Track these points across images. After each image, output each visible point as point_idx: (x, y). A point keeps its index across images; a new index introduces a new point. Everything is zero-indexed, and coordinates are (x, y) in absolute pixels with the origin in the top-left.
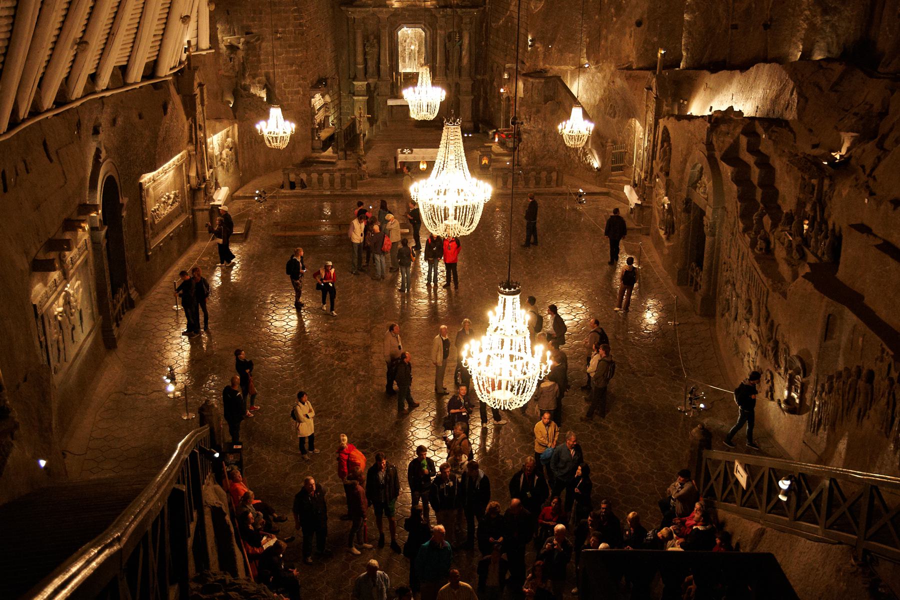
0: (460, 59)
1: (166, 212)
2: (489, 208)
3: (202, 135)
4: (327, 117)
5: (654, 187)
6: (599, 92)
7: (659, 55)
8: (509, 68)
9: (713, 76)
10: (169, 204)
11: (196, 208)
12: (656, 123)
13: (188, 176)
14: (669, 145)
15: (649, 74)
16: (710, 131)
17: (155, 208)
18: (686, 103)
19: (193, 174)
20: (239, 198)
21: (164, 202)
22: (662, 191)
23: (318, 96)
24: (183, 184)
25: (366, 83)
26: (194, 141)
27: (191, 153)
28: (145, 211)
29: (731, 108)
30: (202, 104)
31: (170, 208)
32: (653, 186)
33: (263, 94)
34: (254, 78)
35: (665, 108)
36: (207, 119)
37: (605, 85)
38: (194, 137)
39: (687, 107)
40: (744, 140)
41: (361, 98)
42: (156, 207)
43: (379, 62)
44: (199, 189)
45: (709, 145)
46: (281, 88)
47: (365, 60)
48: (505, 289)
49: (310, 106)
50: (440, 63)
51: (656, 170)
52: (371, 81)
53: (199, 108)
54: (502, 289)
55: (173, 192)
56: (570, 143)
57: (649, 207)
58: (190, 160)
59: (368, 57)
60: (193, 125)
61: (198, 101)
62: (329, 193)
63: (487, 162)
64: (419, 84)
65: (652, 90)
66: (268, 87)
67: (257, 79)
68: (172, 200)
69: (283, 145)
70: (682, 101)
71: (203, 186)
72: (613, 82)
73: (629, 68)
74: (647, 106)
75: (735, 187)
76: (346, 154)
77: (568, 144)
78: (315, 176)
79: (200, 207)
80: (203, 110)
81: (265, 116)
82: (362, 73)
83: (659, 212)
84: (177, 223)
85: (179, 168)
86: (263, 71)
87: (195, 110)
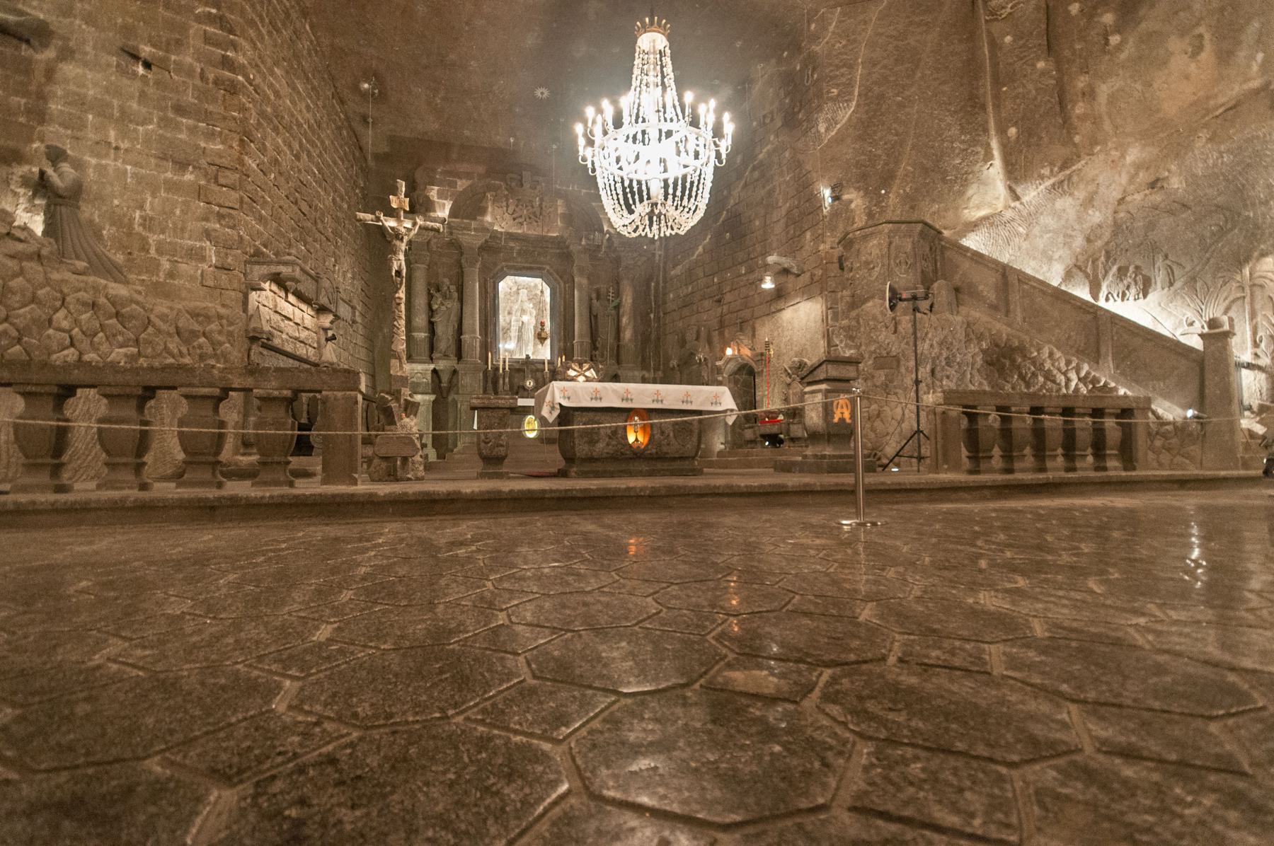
0: (618, 331)
25: (432, 366)
43: (460, 331)
46: (130, 226)
49: (245, 310)
50: (581, 336)
52: (441, 365)
59: (436, 319)
82: (425, 347)
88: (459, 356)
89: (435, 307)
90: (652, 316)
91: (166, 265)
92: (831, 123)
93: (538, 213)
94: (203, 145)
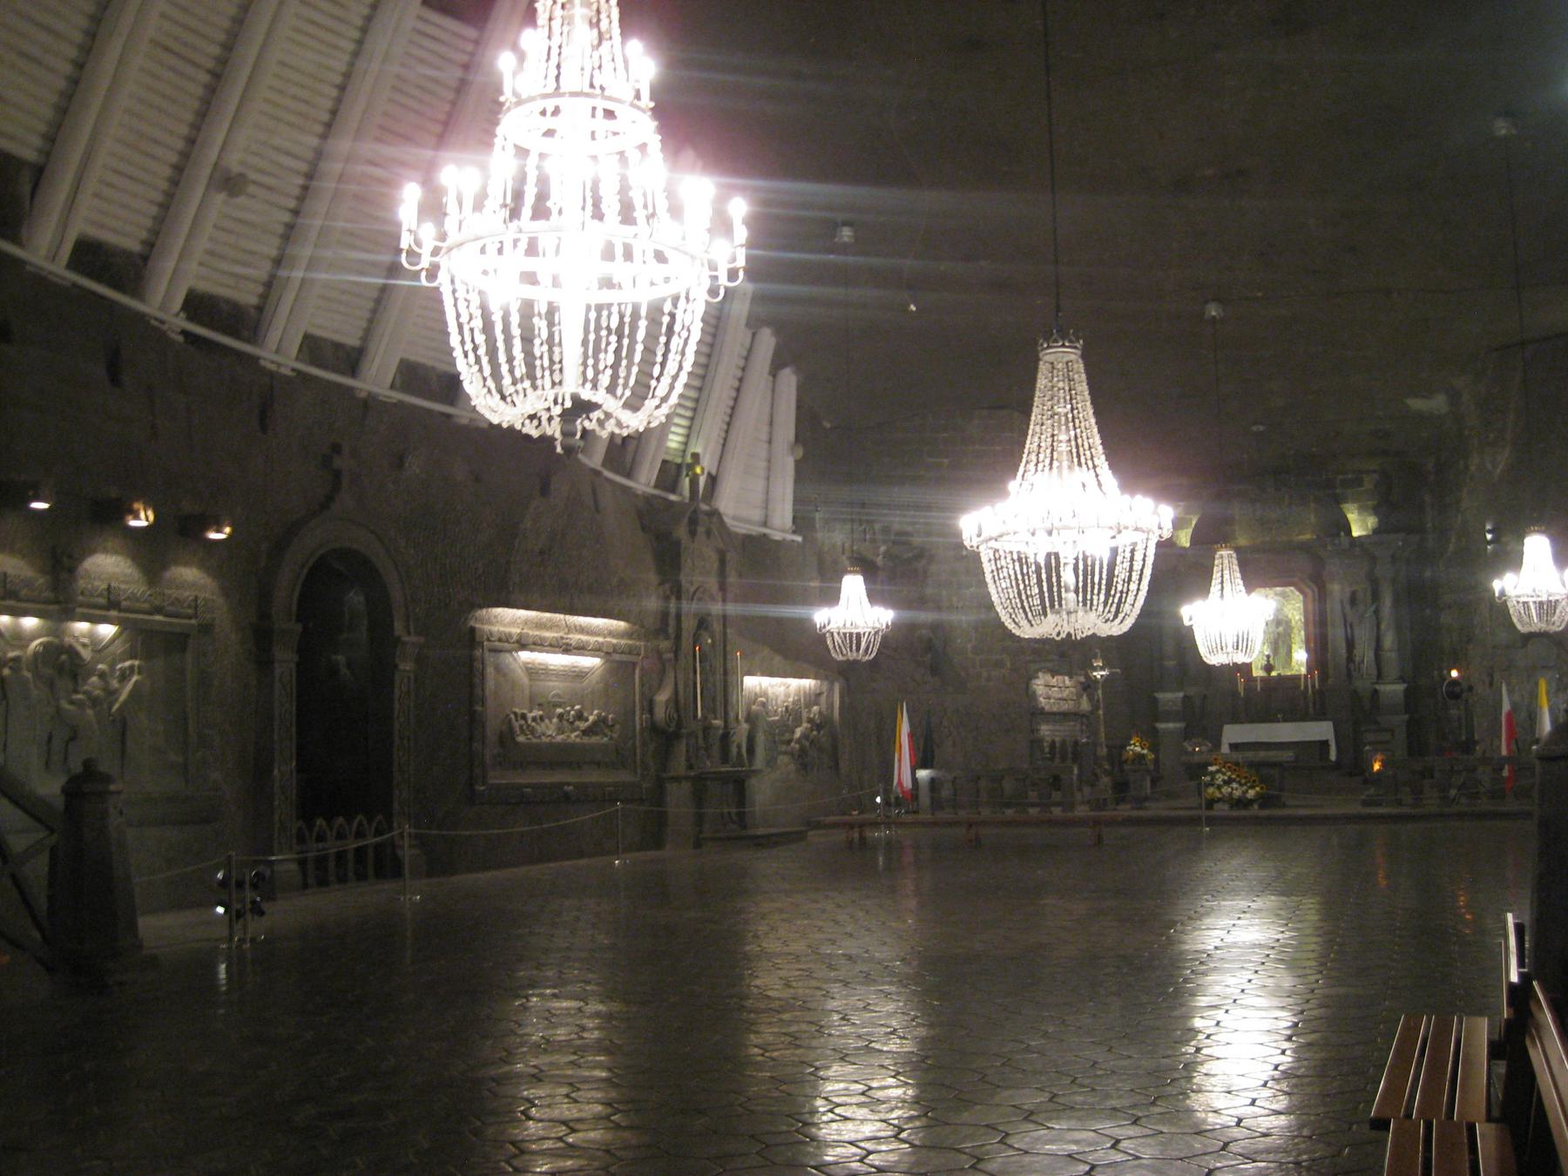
1: (562, 736)
10: (577, 729)
11: (664, 775)
13: (651, 703)
19: (662, 697)
21: (561, 716)
25: (1181, 695)
26: (671, 630)
28: (478, 691)
31: (577, 736)
41: (1171, 725)
68: (587, 724)
81: (831, 596)
84: (593, 777)
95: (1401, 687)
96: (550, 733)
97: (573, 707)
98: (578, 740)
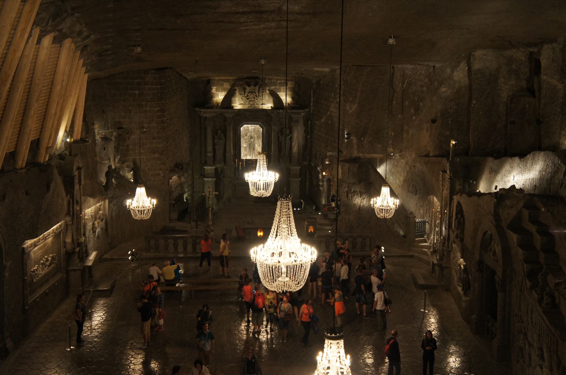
1: (44, 272)
2: (314, 267)
3: (78, 209)
4: (181, 196)
5: (451, 251)
6: (402, 175)
7: (451, 145)
8: (330, 156)
9: (496, 161)
10: (47, 266)
11: (71, 268)
12: (451, 199)
13: (65, 242)
14: (463, 216)
15: (444, 160)
16: (497, 206)
17: (34, 268)
18: (474, 182)
19: (69, 240)
20: (106, 260)
21: (43, 264)
22: (459, 255)
23: (175, 177)
24: (60, 249)
25: (215, 167)
26: (71, 213)
27: (68, 223)
29: (513, 187)
30: (80, 184)
31: (48, 269)
32: (450, 249)
33: (130, 175)
34: (123, 163)
35: (458, 187)
36: (83, 196)
37: (408, 168)
38: (71, 210)
39: (477, 186)
40: (526, 213)
41: (210, 179)
42: (36, 268)
43: (225, 151)
44: (74, 252)
45: (496, 216)
47: (214, 150)
48: (331, 334)
51: (452, 237)
52: (218, 166)
53: (77, 187)
54: (329, 335)
55: (51, 255)
56: (381, 215)
57: (447, 267)
58: (67, 229)
60: (71, 200)
61: (76, 181)
62: (182, 256)
63: (312, 230)
64: (257, 168)
65: (446, 172)
66: (136, 170)
67: (126, 164)
68: (49, 262)
69: (146, 217)
70: (471, 181)
71: (77, 250)
72: (414, 167)
73: (427, 156)
74: (443, 185)
75: (521, 251)
76: (197, 224)
77: (378, 216)
78: (171, 242)
79: (74, 268)
80: (80, 188)
81: (132, 195)
83: (456, 272)
84: (52, 282)
85: (57, 235)
86: (131, 158)
87: (73, 188)
88: (225, 162)
89: (215, 142)
90: (309, 137)
91: (153, 179)
92: (351, 109)
93: (258, 96)
94: (158, 146)
95: (298, 168)
96: (40, 272)
97: (44, 257)
98: (48, 270)
